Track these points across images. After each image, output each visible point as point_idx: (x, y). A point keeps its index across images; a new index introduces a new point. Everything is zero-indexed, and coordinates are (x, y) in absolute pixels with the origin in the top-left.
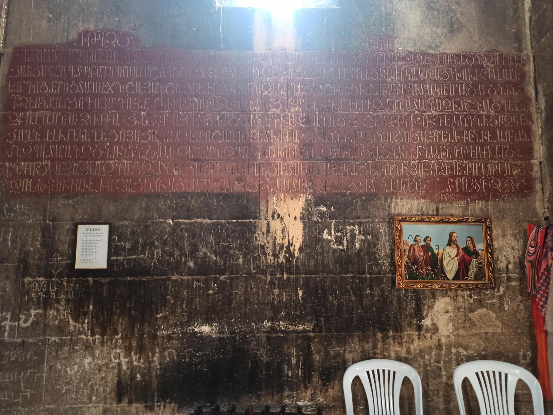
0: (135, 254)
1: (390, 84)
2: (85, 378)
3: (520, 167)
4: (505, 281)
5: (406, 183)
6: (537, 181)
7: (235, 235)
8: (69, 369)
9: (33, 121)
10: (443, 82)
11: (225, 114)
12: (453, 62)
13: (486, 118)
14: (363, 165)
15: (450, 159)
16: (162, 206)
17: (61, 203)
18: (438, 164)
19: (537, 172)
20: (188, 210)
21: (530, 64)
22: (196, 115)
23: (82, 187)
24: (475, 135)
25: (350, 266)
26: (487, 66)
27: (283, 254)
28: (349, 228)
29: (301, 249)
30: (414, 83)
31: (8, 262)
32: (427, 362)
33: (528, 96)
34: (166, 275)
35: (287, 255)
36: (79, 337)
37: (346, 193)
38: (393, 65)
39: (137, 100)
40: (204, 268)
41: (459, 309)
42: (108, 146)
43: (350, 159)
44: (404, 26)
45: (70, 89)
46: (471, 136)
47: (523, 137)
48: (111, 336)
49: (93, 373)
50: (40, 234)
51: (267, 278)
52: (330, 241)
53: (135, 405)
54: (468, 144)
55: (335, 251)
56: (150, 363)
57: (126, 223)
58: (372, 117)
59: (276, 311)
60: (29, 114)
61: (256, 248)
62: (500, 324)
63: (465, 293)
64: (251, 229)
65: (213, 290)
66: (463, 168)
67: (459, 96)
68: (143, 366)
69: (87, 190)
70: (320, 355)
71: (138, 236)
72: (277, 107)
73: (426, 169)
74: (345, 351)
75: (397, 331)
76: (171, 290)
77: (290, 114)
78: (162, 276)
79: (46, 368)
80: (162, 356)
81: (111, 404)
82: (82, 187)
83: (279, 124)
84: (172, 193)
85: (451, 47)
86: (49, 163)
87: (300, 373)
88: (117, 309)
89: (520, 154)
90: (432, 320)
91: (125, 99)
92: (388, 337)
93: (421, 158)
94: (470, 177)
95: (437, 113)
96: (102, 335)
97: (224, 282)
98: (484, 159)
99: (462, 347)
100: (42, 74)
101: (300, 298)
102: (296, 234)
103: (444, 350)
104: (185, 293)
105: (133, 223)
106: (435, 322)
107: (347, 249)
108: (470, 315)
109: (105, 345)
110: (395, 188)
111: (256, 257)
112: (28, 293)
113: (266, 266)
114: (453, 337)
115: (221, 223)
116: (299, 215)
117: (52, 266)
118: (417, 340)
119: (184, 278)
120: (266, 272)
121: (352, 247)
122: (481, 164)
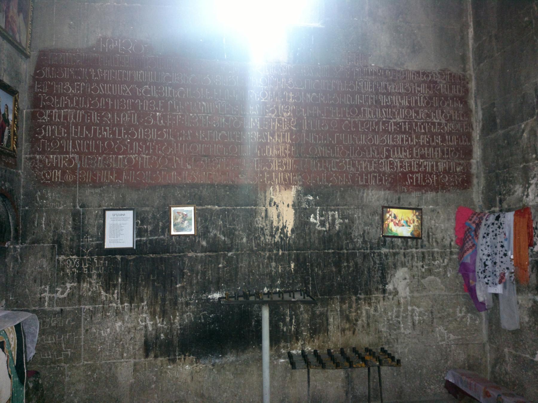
2: (116, 339)
3: (462, 165)
4: (449, 255)
5: (376, 177)
6: (475, 177)
7: (239, 219)
8: (102, 332)
9: (59, 117)
10: (406, 94)
11: (229, 117)
12: (414, 78)
13: (438, 125)
16: (178, 195)
17: (88, 192)
18: (401, 162)
19: (475, 169)
20: (200, 198)
27: (279, 235)
28: (330, 213)
29: (293, 231)
30: (383, 94)
31: (43, 243)
32: (390, 318)
34: (183, 253)
35: (282, 235)
36: (110, 305)
38: (367, 78)
39: (153, 102)
40: (215, 247)
41: (414, 276)
42: (128, 143)
45: (91, 90)
47: (465, 141)
48: (138, 303)
49: (123, 335)
50: (71, 219)
51: (266, 254)
52: (316, 224)
53: (160, 359)
54: (424, 146)
55: (319, 232)
56: (171, 324)
57: (148, 209)
59: (273, 280)
60: (55, 112)
62: (444, 288)
64: (252, 214)
66: (419, 166)
67: (418, 106)
68: (166, 327)
70: (308, 314)
71: (158, 220)
74: (327, 310)
75: (367, 294)
77: (283, 118)
78: (179, 253)
79: (83, 331)
80: (181, 318)
81: (140, 359)
82: (107, 179)
83: (274, 126)
84: (186, 184)
85: (412, 65)
87: (293, 329)
88: (142, 281)
89: (463, 154)
90: (394, 285)
91: (142, 101)
92: (359, 299)
93: (388, 157)
94: (425, 172)
96: (131, 303)
97: (231, 257)
98: (435, 159)
99: (416, 306)
102: (289, 218)
103: (403, 308)
104: (199, 267)
105: (154, 209)
106: (396, 286)
107: (329, 230)
108: (422, 281)
109: (133, 311)
110: (367, 182)
111: (257, 237)
112: (63, 269)
113: (265, 244)
114: (409, 298)
115: (228, 209)
116: (291, 203)
117: (83, 246)
118: (382, 301)
119: (199, 254)
120: (265, 249)
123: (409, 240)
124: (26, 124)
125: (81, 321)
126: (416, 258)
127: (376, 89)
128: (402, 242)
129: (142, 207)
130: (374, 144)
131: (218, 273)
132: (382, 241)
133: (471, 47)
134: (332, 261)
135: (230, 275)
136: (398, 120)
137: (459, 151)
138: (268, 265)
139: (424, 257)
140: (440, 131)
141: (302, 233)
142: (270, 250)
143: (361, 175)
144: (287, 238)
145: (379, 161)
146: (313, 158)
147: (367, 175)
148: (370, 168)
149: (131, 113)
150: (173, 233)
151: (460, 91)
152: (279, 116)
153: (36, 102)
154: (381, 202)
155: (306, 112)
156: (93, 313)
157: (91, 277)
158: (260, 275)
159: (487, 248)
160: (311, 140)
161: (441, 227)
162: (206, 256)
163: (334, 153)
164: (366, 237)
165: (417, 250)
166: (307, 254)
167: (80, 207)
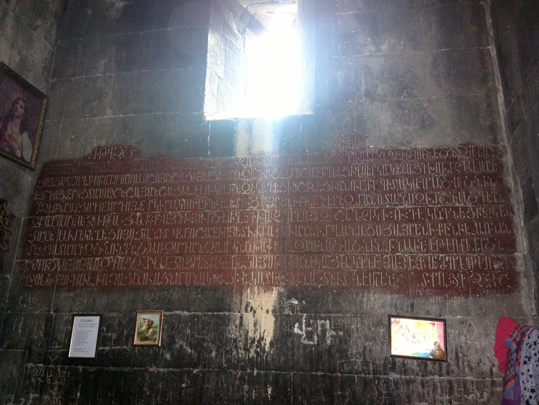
0: (119, 345)
1: (362, 180)
3: (501, 260)
5: (379, 277)
6: (522, 276)
7: (209, 328)
9: (50, 224)
10: (415, 176)
12: (425, 157)
14: (335, 258)
17: (63, 295)
18: (412, 257)
19: (521, 266)
21: (507, 155)
23: (82, 280)
24: (451, 228)
25: (321, 364)
26: (462, 159)
27: (254, 349)
28: (319, 322)
29: (271, 344)
30: (385, 178)
35: (258, 350)
37: (317, 286)
38: (365, 162)
39: (135, 202)
40: (180, 360)
42: (107, 244)
43: (322, 253)
44: (375, 126)
45: (81, 195)
46: (447, 229)
47: (504, 229)
50: (44, 324)
51: (238, 373)
52: (301, 336)
54: (443, 237)
55: (305, 346)
57: (115, 314)
58: (344, 212)
60: (48, 218)
61: (228, 341)
65: (186, 384)
66: (439, 262)
67: (433, 189)
69: (85, 284)
73: (400, 263)
76: (148, 382)
77: (266, 211)
78: (141, 367)
82: (82, 282)
84: (157, 286)
85: (423, 142)
86: (59, 260)
89: (502, 246)
91: (125, 203)
93: (394, 251)
94: (447, 271)
95: (409, 207)
97: (197, 375)
98: (461, 252)
100: (61, 184)
101: (269, 396)
105: (120, 315)
107: (318, 345)
110: (367, 281)
111: (228, 351)
113: (237, 360)
115: (198, 315)
116: (271, 309)
119: (161, 370)
120: (237, 366)
121: (323, 343)
122: (459, 258)
123: (429, 362)
124: (22, 231)
126: (439, 388)
127: (376, 173)
128: (419, 365)
129: (109, 312)
130: (375, 236)
131: (180, 395)
132: (389, 363)
133: (501, 114)
134: (321, 387)
136: (406, 206)
137: (495, 242)
138: (240, 388)
139: (451, 388)
140: (466, 218)
142: (243, 369)
143: (360, 273)
144: (264, 354)
145: (382, 256)
146: (299, 253)
147: (367, 274)
148: (371, 265)
149: (113, 215)
150: (136, 341)
151: (490, 168)
152: (261, 208)
153: (34, 211)
154: (388, 309)
155: (292, 203)
160: (298, 234)
162: (168, 372)
163: (324, 248)
164: (367, 355)
165: (442, 378)
166: (288, 376)
167: (54, 312)
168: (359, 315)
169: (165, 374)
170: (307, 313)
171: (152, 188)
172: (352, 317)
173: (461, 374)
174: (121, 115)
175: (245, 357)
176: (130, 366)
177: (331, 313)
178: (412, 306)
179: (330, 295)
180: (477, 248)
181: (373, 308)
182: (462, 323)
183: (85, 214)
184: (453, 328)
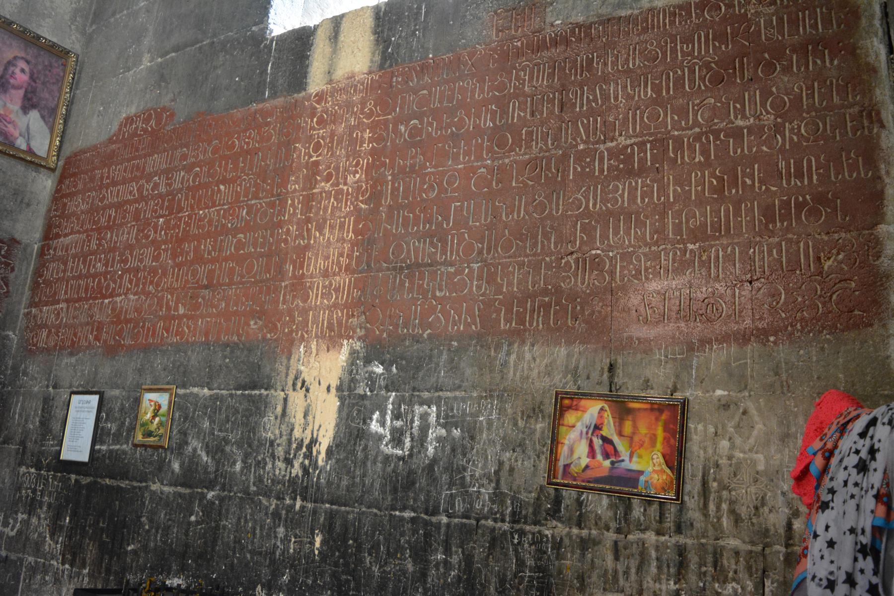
0: (118, 443)
5: (547, 306)
12: (672, 23)
15: (656, 244)
22: (219, 215)
24: (721, 180)
27: (301, 460)
28: (418, 410)
29: (329, 452)
33: (868, 64)
35: (307, 462)
37: (421, 335)
40: (191, 477)
46: (711, 183)
47: (853, 167)
52: (380, 438)
55: (387, 458)
61: (262, 444)
63: (664, 587)
72: (328, 179)
77: (345, 188)
78: (141, 482)
84: (171, 345)
95: (628, 142)
96: (72, 566)
100: (80, 186)
101: (317, 552)
104: (162, 516)
107: (411, 456)
111: (259, 462)
113: (273, 480)
115: (222, 395)
116: (334, 383)
119: (166, 489)
120: (271, 491)
121: (420, 452)
125: (19, 582)
128: (611, 506)
129: (112, 388)
130: (550, 216)
131: (187, 534)
134: (408, 542)
135: (205, 543)
139: (682, 565)
140: (759, 151)
141: (347, 458)
146: (395, 268)
150: (139, 437)
151: (827, 22)
152: (338, 184)
153: (49, 234)
154: (557, 378)
156: (33, 570)
157: (41, 508)
158: (253, 552)
159: (826, 552)
161: (754, 463)
164: (502, 482)
165: (663, 539)
166: (351, 517)
168: (496, 394)
169: (171, 496)
170: (397, 391)
171: (182, 174)
172: (482, 397)
173: (711, 532)
174: (159, 60)
175: (285, 476)
176: (127, 479)
177: (442, 390)
178: (612, 368)
179: (445, 353)
180: (782, 222)
181: (528, 378)
182: (726, 407)
183: (99, 230)
184: (701, 419)
